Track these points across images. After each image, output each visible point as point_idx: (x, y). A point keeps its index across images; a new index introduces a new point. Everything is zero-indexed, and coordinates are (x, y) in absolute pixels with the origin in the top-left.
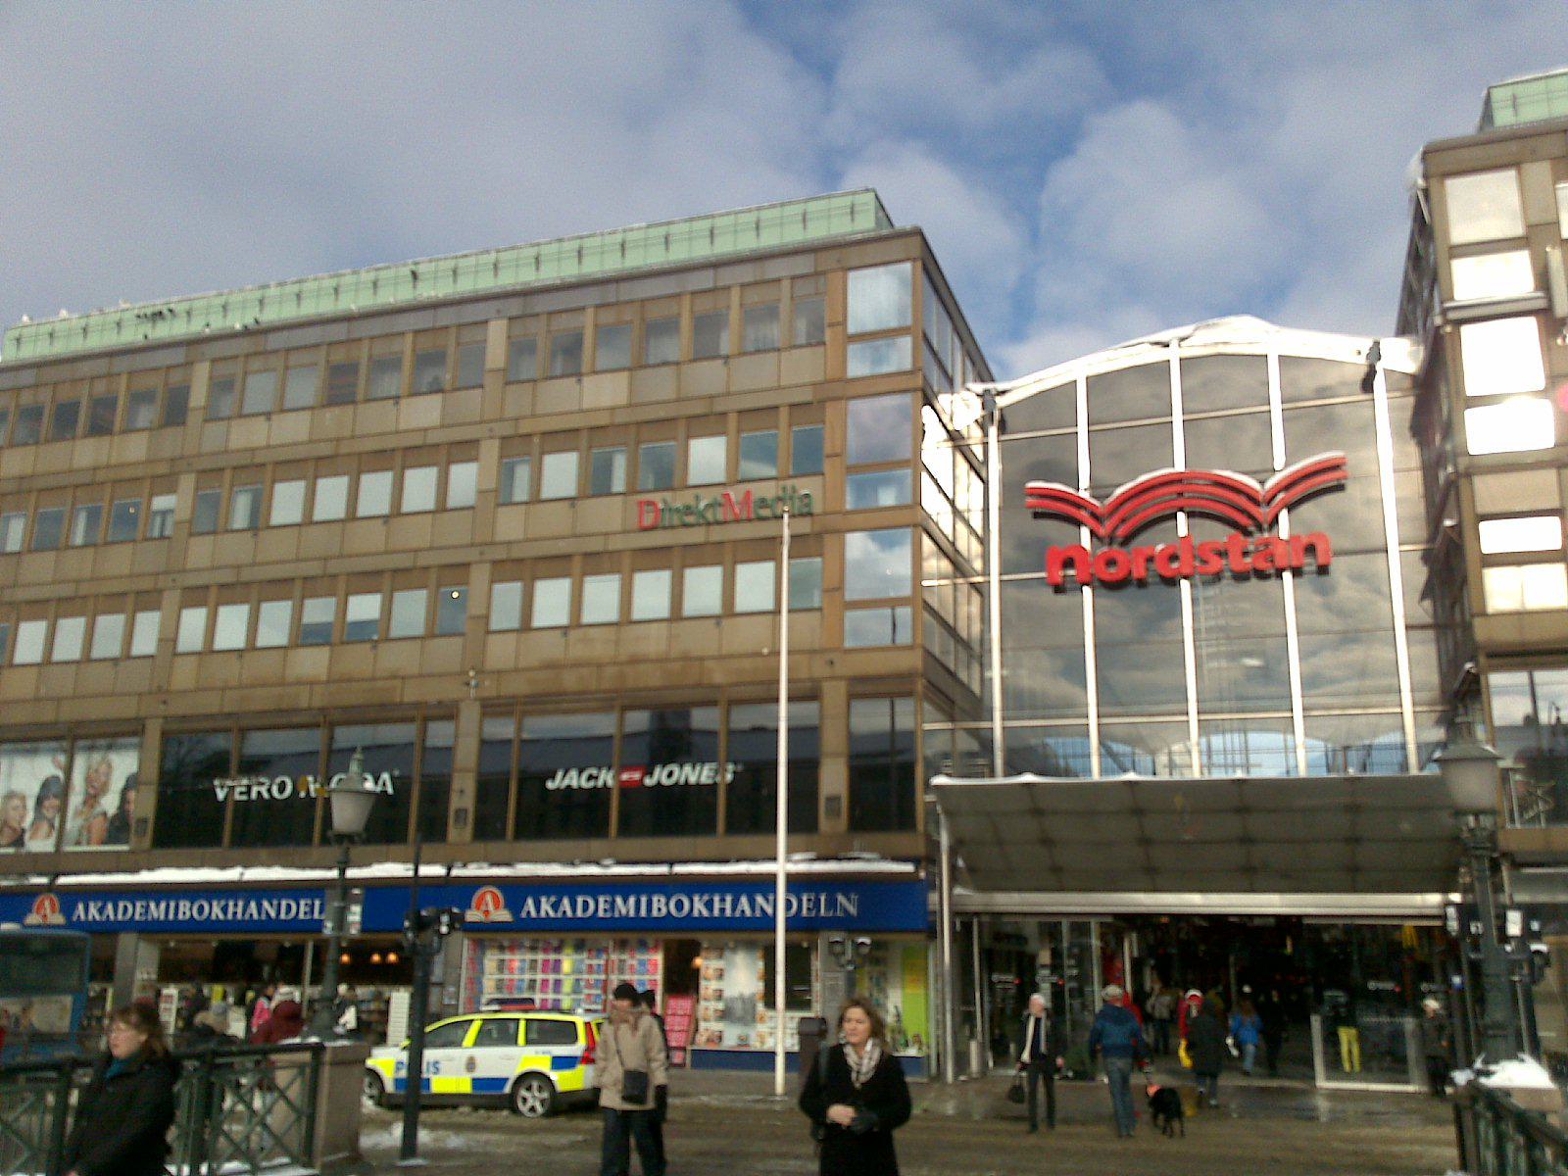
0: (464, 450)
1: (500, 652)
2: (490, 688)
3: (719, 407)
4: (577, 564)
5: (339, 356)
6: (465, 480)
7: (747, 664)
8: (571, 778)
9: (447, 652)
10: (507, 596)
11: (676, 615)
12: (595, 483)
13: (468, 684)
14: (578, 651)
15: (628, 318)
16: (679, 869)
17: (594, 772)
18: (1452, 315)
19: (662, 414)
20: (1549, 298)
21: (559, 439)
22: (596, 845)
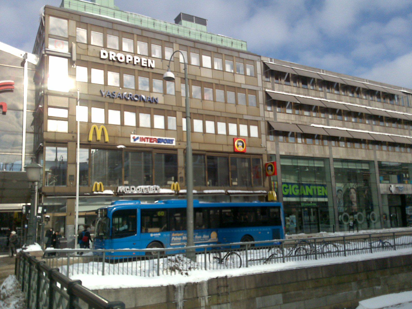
18: (47, 52)
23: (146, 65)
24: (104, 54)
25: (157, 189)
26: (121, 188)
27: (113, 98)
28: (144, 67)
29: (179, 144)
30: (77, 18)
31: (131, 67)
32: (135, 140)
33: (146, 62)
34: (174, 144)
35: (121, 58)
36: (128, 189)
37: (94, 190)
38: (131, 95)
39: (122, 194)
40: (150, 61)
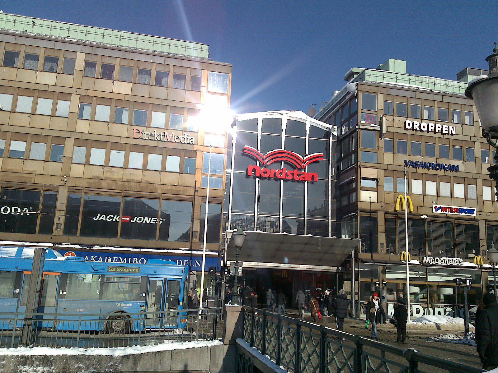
0: (66, 96)
1: (77, 171)
2: (72, 183)
3: (164, 103)
4: (109, 145)
5: (10, 48)
6: (63, 107)
7: (169, 187)
8: (103, 218)
9: (55, 168)
10: (79, 153)
11: (145, 168)
12: (116, 119)
13: (63, 180)
14: (108, 175)
15: (132, 65)
16: (142, 250)
17: (112, 216)
18: (361, 127)
19: (143, 101)
20: (381, 128)
21: (104, 100)
22: (112, 241)
23: (447, 132)
24: (409, 124)
25: (461, 261)
26: (426, 259)
27: (416, 168)
28: (445, 134)
29: (481, 215)
30: (384, 91)
31: (432, 135)
32: (437, 209)
33: (447, 129)
34: (475, 215)
35: (424, 127)
36: (432, 260)
37: (402, 259)
38: (433, 164)
39: (427, 264)
40: (451, 128)
